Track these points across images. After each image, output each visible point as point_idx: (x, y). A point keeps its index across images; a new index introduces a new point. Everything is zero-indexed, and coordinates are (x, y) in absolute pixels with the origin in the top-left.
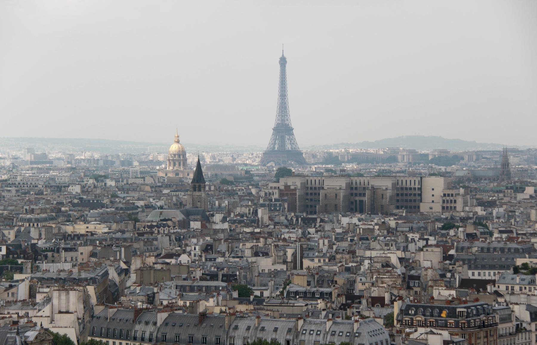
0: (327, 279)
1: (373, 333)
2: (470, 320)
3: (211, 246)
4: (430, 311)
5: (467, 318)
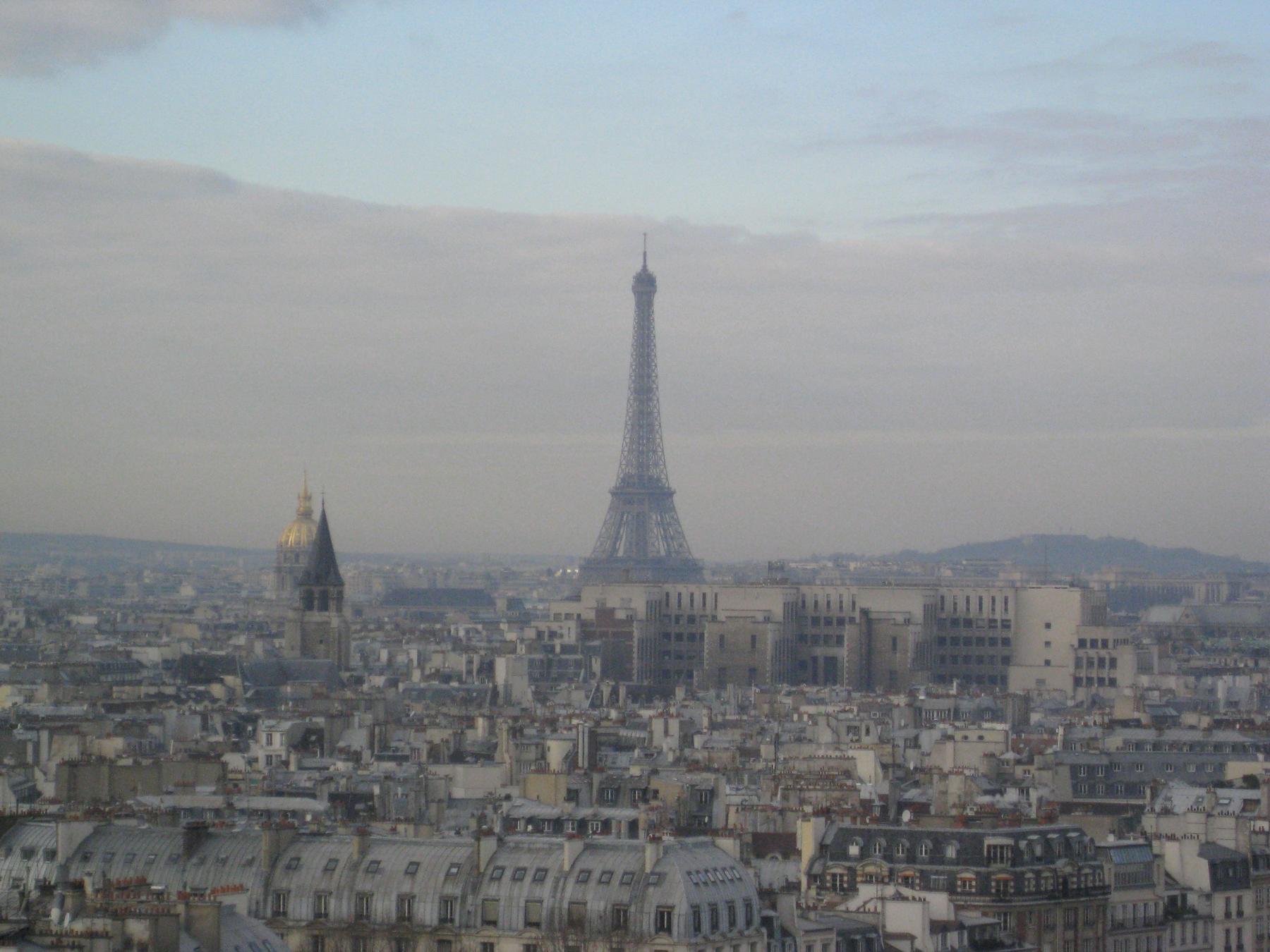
0: (630, 786)
1: (702, 877)
2: (1023, 873)
3: (319, 732)
4: (907, 845)
5: (1013, 865)
